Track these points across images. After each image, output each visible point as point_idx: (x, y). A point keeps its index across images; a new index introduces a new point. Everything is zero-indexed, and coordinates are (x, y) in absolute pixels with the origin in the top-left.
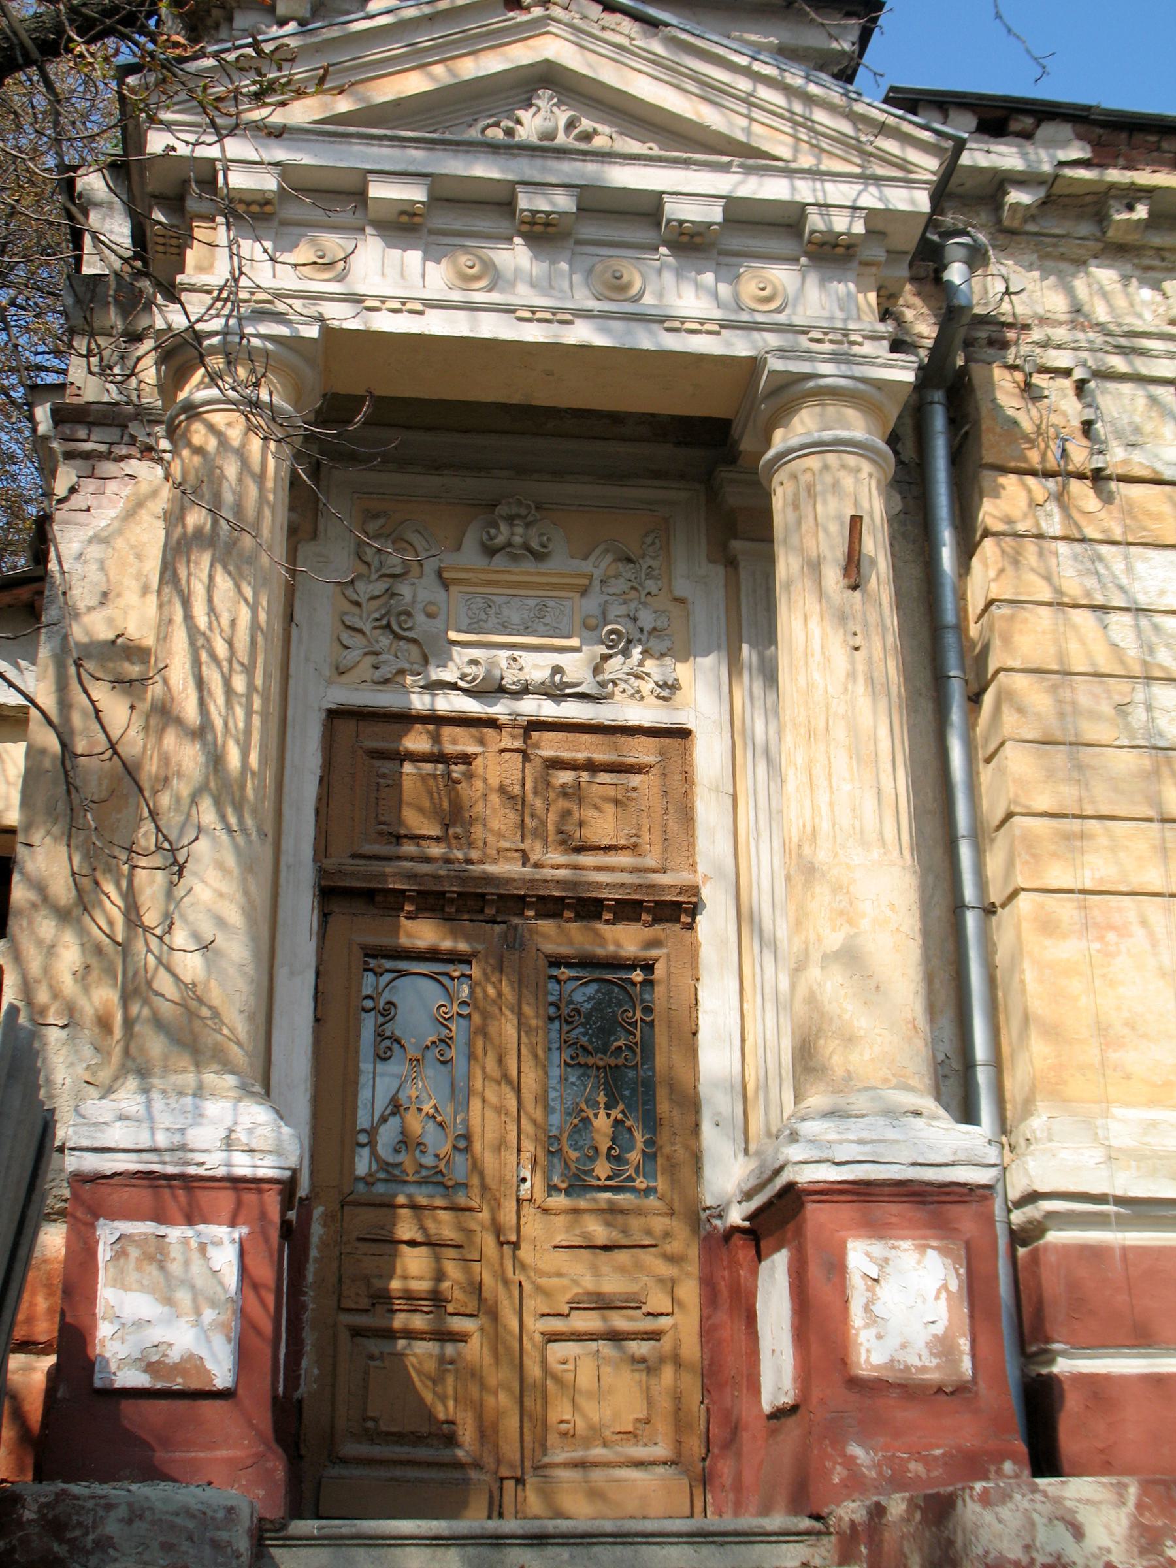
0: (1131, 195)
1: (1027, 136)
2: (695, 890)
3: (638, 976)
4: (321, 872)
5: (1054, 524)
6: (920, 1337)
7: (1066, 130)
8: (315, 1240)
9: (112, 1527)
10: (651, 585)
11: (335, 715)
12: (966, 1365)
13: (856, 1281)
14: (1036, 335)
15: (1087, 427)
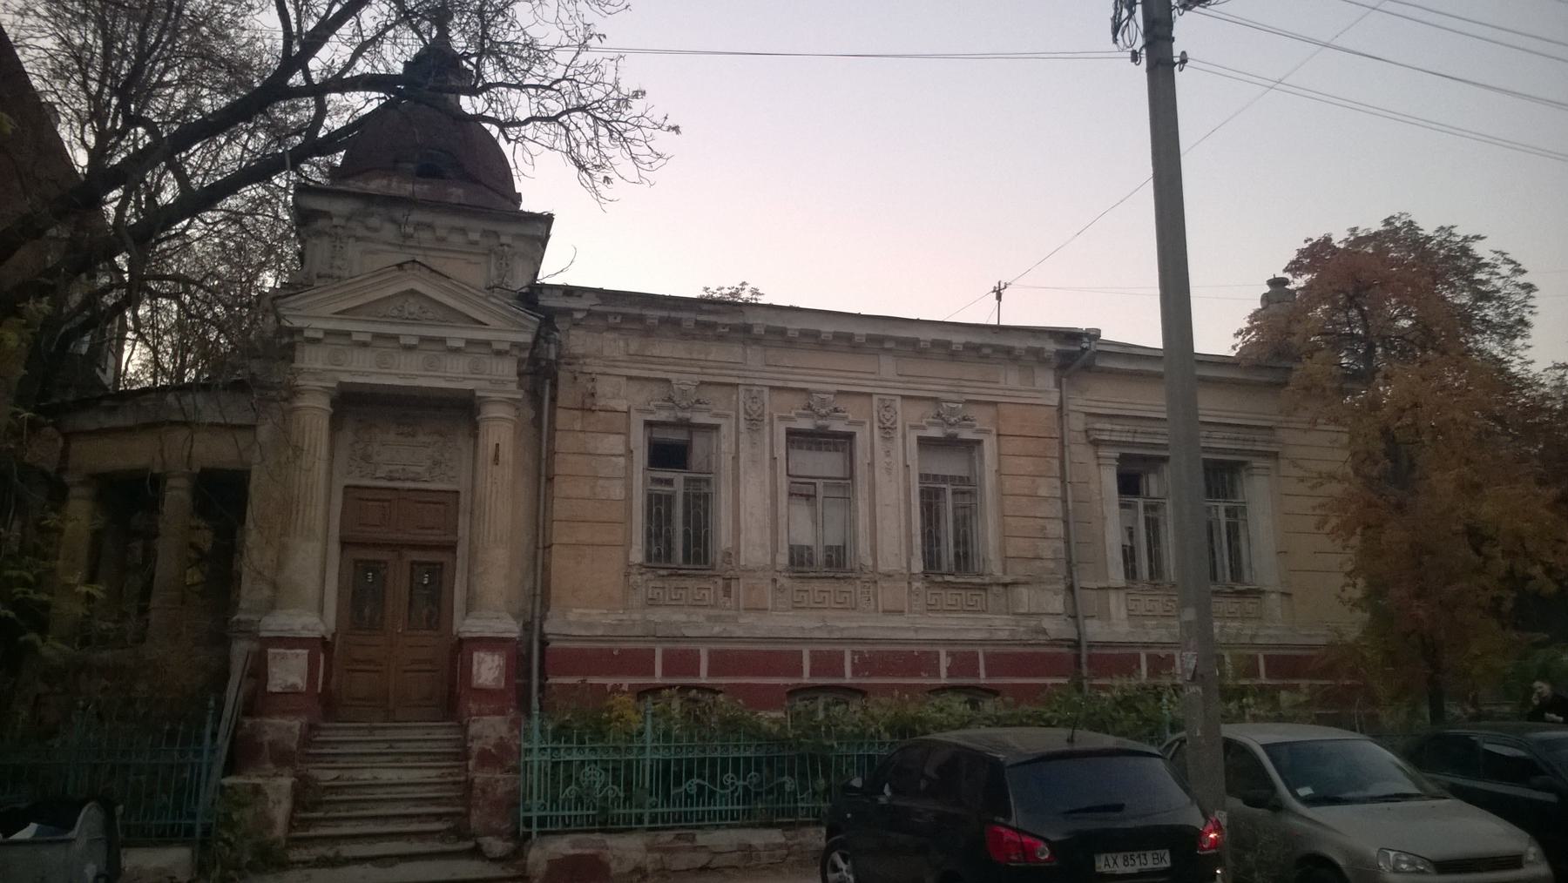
0: (616, 314)
1: (580, 296)
2: (456, 543)
3: (438, 567)
4: (341, 537)
5: (578, 427)
6: (490, 679)
7: (593, 295)
8: (337, 644)
9: (267, 728)
10: (450, 444)
11: (347, 487)
12: (503, 684)
13: (475, 663)
14: (581, 362)
15: (593, 395)
